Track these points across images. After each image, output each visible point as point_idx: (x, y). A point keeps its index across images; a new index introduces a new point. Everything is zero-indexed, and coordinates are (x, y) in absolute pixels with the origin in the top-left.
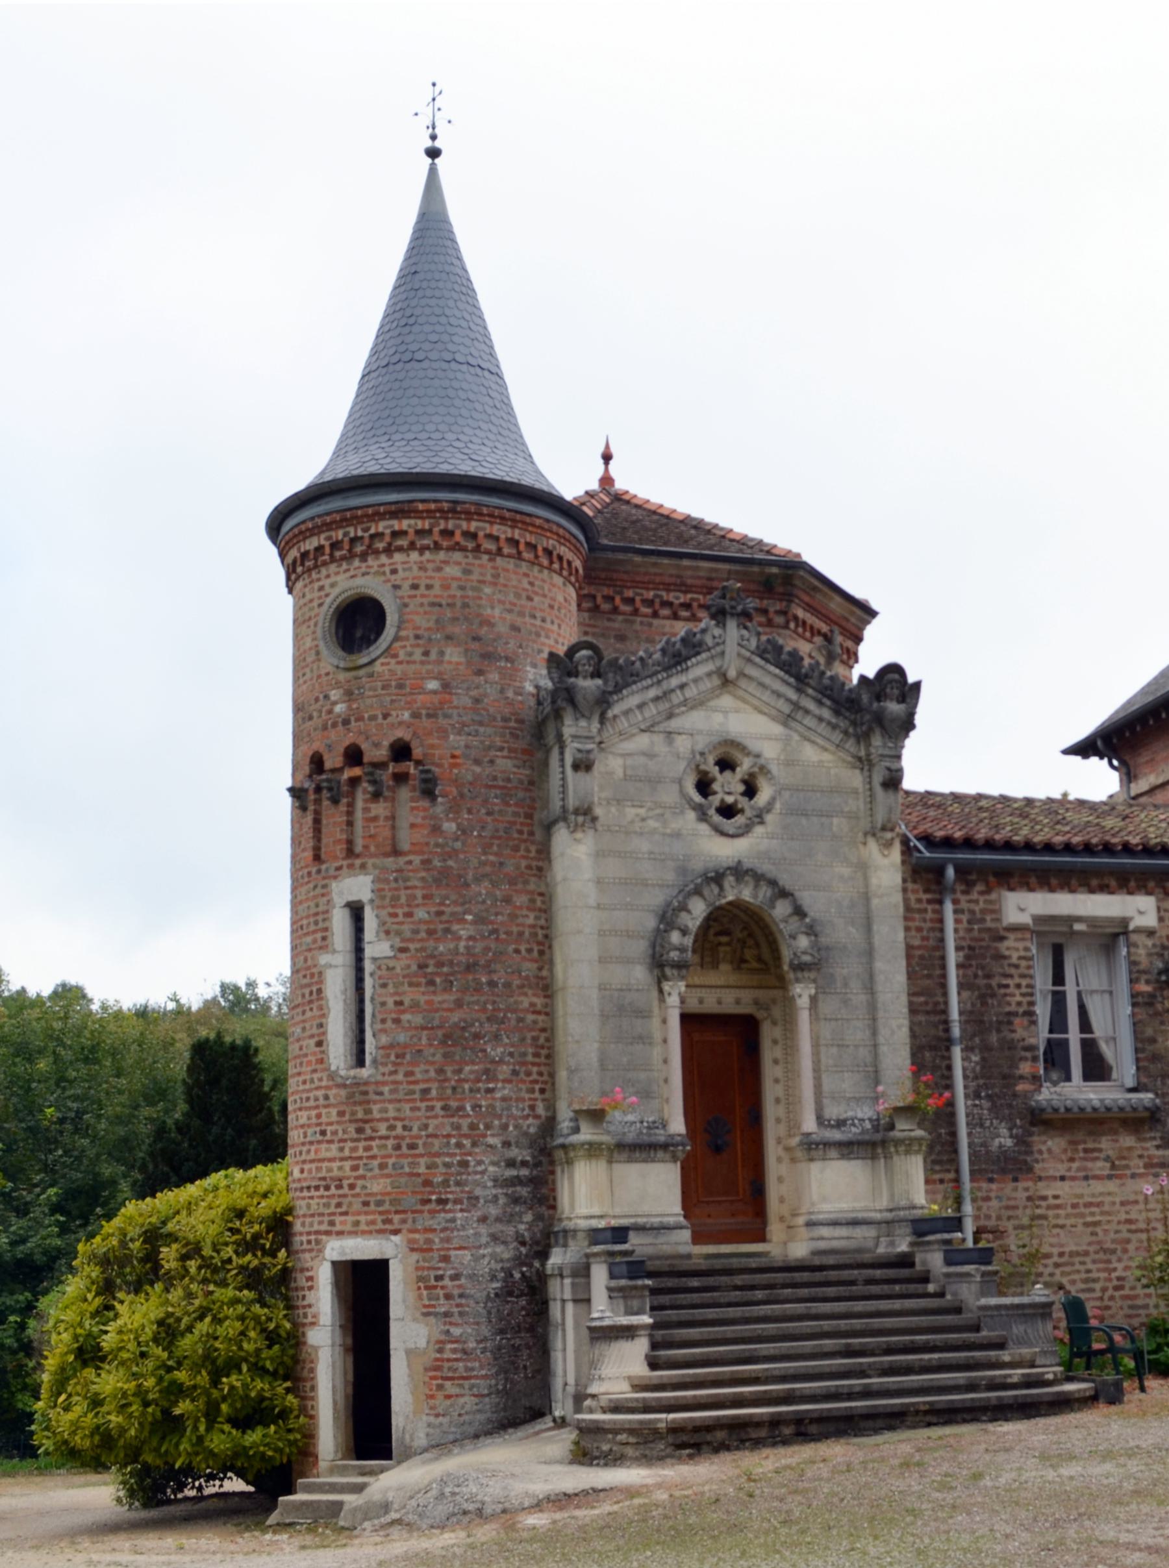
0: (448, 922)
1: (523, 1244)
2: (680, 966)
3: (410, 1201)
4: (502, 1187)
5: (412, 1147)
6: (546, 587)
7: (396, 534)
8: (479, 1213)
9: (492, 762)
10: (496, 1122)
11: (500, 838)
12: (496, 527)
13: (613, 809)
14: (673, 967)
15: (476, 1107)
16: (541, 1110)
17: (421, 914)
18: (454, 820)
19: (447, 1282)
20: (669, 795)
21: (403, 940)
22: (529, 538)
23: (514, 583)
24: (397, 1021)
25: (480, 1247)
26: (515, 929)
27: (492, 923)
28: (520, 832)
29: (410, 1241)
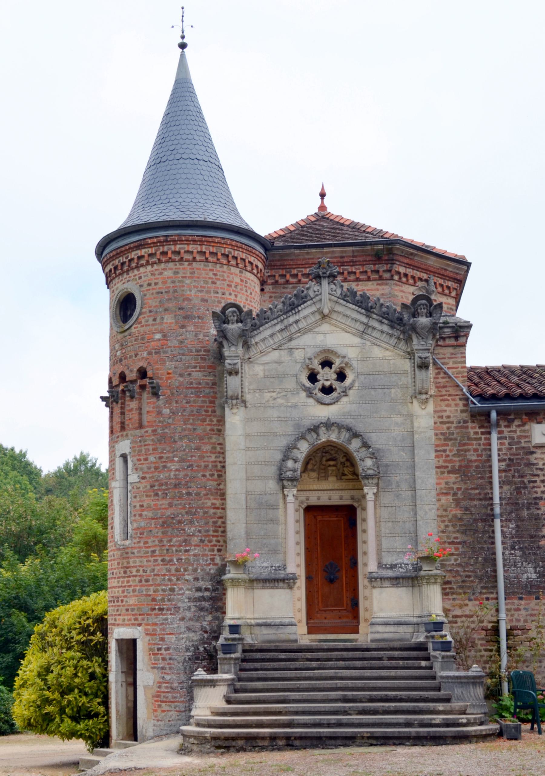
0: (165, 462)
1: (206, 632)
2: (292, 480)
3: (146, 609)
4: (193, 602)
5: (147, 581)
6: (225, 275)
7: (140, 258)
8: (180, 616)
9: (189, 374)
10: (190, 568)
11: (194, 415)
12: (191, 246)
13: (257, 395)
14: (288, 480)
15: (179, 560)
16: (218, 560)
17: (152, 459)
18: (169, 407)
19: (163, 651)
20: (290, 384)
21: (144, 473)
22: (211, 249)
23: (204, 275)
24: (141, 515)
25: (180, 633)
26: (203, 464)
27: (189, 461)
28: (207, 411)
29: (146, 630)
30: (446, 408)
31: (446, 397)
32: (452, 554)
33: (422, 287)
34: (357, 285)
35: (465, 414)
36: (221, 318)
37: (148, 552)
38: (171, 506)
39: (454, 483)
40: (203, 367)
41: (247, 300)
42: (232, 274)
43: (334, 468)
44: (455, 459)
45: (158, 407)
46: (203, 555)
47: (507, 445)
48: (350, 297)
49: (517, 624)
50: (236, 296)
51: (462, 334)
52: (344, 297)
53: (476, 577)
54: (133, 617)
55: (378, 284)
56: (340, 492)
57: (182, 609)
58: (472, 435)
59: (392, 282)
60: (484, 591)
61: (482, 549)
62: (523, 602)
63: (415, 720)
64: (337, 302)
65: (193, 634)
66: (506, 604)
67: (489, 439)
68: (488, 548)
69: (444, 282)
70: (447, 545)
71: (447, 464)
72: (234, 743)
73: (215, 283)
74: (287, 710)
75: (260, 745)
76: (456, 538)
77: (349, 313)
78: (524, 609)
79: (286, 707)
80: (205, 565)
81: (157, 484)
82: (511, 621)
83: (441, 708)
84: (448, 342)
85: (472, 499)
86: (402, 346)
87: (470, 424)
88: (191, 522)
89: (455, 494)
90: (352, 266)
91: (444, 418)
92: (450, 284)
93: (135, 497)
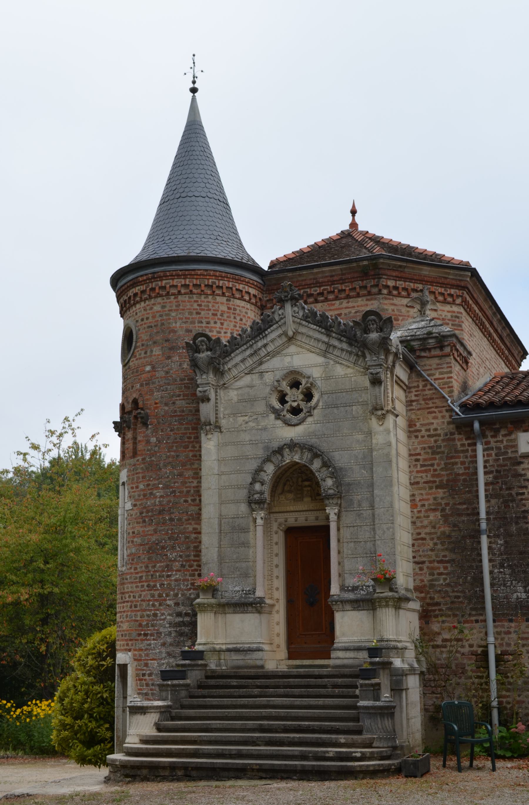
0: (151, 489)
2: (261, 502)
3: (134, 634)
4: (174, 627)
5: (136, 606)
6: (210, 305)
8: (162, 641)
9: (174, 403)
10: (172, 593)
11: (177, 442)
12: (175, 280)
13: (231, 419)
14: (255, 503)
15: (162, 585)
17: (141, 486)
18: (155, 436)
19: (147, 677)
20: (261, 407)
21: (136, 500)
22: (195, 281)
23: (188, 307)
24: (132, 542)
25: (161, 659)
26: (185, 490)
27: (172, 487)
28: (189, 438)
29: (134, 655)
30: (433, 421)
31: (433, 410)
32: (440, 574)
33: (416, 298)
34: (348, 302)
35: (452, 426)
36: (193, 348)
37: (136, 578)
38: (156, 533)
39: (442, 498)
40: (187, 395)
41: (235, 326)
42: (217, 303)
43: (309, 489)
44: (442, 473)
45: (147, 436)
46: (184, 580)
47: (494, 456)
48: (311, 318)
49: (508, 649)
50: (222, 324)
51: (446, 344)
52: (305, 318)
53: (465, 597)
54: (125, 643)
55: (367, 300)
56: (315, 512)
57: (163, 635)
58: (459, 448)
59: (381, 296)
60: (474, 613)
61: (471, 567)
62: (513, 625)
63: (310, 752)
64: (300, 324)
65: (173, 659)
66: (495, 627)
67: (475, 451)
68: (477, 567)
69: (445, 290)
70: (436, 564)
71: (435, 479)
72: (139, 773)
73: (199, 314)
74: (201, 739)
75: (162, 774)
76: (445, 556)
77: (311, 333)
78: (515, 632)
79: (200, 736)
80: (185, 590)
81: (145, 510)
82: (501, 645)
83: (343, 741)
84: (433, 353)
85: (460, 515)
86: (361, 362)
87: (457, 436)
88: (173, 548)
89: (443, 510)
90: (341, 284)
91: (432, 431)
92: (452, 291)
93: (129, 524)
